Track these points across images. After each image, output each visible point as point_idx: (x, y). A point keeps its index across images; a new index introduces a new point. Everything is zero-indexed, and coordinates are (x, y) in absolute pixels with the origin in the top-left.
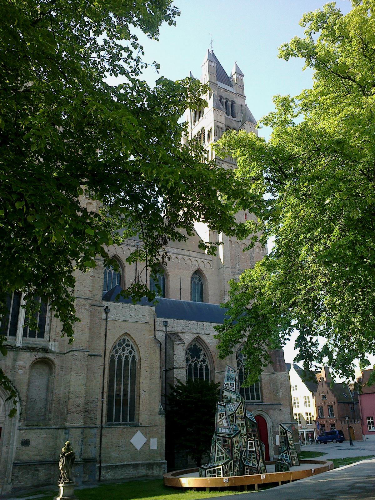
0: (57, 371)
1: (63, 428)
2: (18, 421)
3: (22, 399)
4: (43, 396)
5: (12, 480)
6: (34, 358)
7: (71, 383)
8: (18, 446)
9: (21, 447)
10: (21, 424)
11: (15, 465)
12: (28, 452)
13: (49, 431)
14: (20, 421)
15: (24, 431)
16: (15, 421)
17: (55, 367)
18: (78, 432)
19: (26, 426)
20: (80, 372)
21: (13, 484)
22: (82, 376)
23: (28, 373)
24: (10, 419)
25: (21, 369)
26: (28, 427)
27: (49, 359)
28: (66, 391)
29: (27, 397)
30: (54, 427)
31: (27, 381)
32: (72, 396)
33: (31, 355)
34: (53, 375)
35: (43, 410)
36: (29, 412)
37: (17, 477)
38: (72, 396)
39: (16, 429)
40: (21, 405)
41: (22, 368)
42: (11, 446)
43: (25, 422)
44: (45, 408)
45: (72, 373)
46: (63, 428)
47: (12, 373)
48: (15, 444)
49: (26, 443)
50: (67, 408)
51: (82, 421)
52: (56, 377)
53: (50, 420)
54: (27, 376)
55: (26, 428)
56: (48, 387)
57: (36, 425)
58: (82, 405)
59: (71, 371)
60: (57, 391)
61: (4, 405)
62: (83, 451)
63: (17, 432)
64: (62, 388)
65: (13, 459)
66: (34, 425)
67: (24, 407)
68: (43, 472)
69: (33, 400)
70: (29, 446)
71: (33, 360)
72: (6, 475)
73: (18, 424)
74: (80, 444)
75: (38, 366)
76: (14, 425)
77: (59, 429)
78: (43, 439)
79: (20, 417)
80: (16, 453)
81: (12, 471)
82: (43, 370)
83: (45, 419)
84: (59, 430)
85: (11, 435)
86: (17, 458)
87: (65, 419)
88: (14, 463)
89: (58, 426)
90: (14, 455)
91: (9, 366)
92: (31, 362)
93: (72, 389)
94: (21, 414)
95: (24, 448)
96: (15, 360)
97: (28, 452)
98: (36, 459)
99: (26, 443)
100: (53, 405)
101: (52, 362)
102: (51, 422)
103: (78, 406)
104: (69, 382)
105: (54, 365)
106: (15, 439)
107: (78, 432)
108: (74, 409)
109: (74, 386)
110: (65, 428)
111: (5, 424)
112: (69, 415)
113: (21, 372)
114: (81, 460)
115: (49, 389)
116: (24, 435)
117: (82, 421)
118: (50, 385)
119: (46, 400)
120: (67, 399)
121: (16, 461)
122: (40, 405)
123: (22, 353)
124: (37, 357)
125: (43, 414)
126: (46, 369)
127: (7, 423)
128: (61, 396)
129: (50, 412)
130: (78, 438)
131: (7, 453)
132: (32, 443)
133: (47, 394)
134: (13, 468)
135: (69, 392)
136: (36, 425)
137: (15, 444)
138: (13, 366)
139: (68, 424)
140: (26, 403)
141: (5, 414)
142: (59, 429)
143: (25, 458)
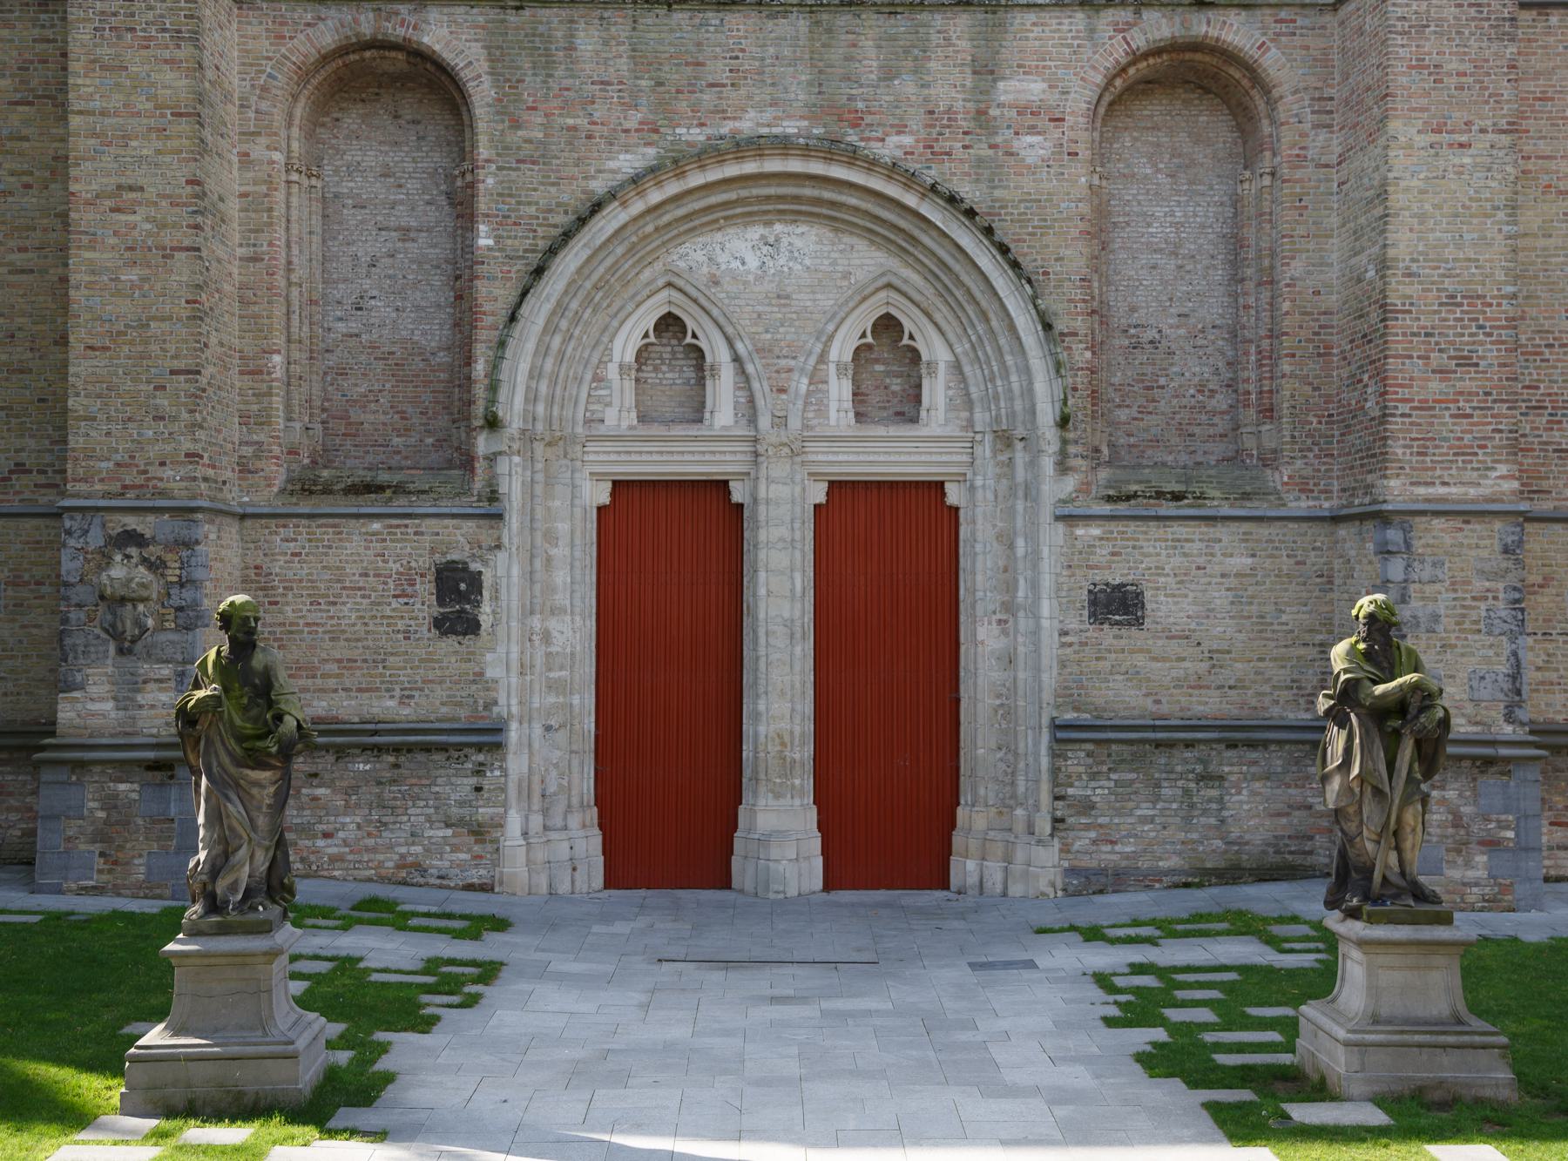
0: (1287, 136)
1: (1362, 517)
2: (1048, 464)
3: (1060, 326)
4: (1213, 310)
5: (1057, 821)
6: (1119, 53)
7: (1397, 199)
8: (1073, 624)
9: (1092, 632)
10: (1070, 483)
11: (1064, 734)
12: (1140, 660)
13: (1263, 531)
14: (1063, 467)
15: (1096, 532)
16: (1033, 464)
17: (1272, 103)
18: (1484, 541)
19: (1109, 499)
20: (1459, 116)
21: (1065, 849)
22: (1481, 143)
23: (1084, 154)
24: (1003, 458)
25: (1032, 130)
26: (1122, 509)
27: (1229, 56)
28: (1362, 259)
29: (1099, 313)
30: (1302, 506)
31: (1084, 208)
32: (1414, 290)
33: (1092, 31)
34: (1267, 162)
35: (1221, 401)
36: (1123, 415)
37: (1087, 807)
38: (1414, 290)
39: (1046, 514)
40: (1058, 366)
41: (1042, 122)
42: (1024, 623)
43: (1104, 474)
44: (1231, 385)
45: (1395, 126)
46: (1362, 517)
47: (980, 161)
48: (1053, 611)
49: (1117, 604)
50: (1381, 376)
51: (1503, 469)
52: (1285, 171)
53: (1269, 460)
54: (1081, 177)
55: (1107, 509)
56: (1235, 245)
57: (1177, 497)
58: (1490, 354)
59: (1384, 119)
60: (1297, 267)
61: (957, 367)
62: (1530, 675)
63: (1053, 536)
64: (1335, 250)
65: (1047, 696)
66: (1159, 495)
67: (1081, 379)
68: (1253, 793)
69: (1152, 334)
70: (1139, 622)
71: (1109, 63)
72: (1021, 789)
73: (1055, 488)
74: (1499, 627)
75: (1153, 109)
76: (1030, 492)
77: (1336, 520)
78: (1232, 582)
79: (1064, 442)
80: (1063, 664)
81: (1055, 771)
82: (1185, 132)
83: (1235, 459)
84: (1343, 531)
85: (1020, 552)
86: (1065, 695)
87: (1375, 457)
88: (1056, 727)
89: (1327, 506)
90: (1050, 679)
91: (949, 110)
92: (1099, 79)
93: (1403, 242)
94: (1064, 422)
95: (1108, 635)
96: (986, 71)
97: (1140, 660)
98: (1199, 709)
99: (1117, 604)
100: (1286, 367)
101: (1251, 70)
102: (1279, 478)
103: (1466, 362)
104: (1382, 194)
105: (1266, 91)
106: (1047, 582)
107: (1484, 541)
108: (1435, 385)
109: (1422, 217)
110: (1383, 518)
111: (972, 488)
112: (1395, 424)
113: (1033, 148)
114: (1521, 734)
115: (1245, 258)
116: (1102, 553)
117: (1503, 469)
118: (1250, 233)
119: (1233, 334)
120: (1374, 317)
121: (1070, 716)
122: (1193, 369)
123: (1031, 17)
124: (1139, 41)
125: (1222, 424)
126: (1215, 126)
127: (986, 478)
128: (1333, 301)
129: (1269, 412)
130: (1480, 585)
131: (1009, 660)
132: (1162, 606)
133: (1235, 296)
134: (1054, 755)
135: (1383, 265)
136: (1177, 497)
137: (1046, 608)
138: (981, 113)
139: (1396, 490)
140: (1092, 348)
141: (970, 424)
142: (1336, 520)
143: (1122, 697)
